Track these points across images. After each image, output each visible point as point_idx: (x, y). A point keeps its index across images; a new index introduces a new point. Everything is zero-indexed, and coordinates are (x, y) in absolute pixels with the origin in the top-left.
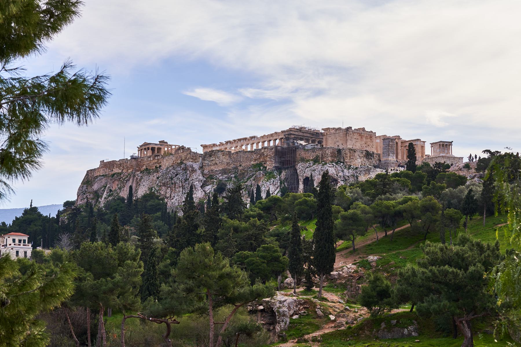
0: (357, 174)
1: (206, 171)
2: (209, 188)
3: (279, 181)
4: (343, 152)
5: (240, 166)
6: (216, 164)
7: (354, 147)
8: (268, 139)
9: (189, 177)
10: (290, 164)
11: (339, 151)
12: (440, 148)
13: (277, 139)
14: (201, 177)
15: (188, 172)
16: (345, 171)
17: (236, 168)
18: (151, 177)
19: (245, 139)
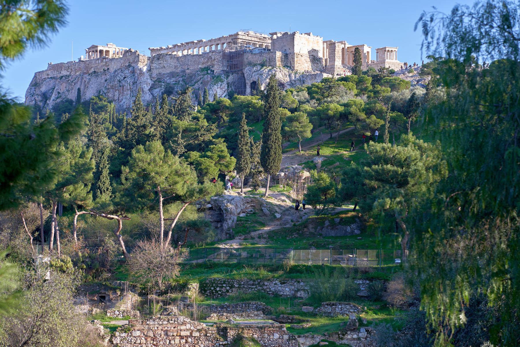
1: (154, 75)
2: (157, 92)
3: (226, 85)
4: (290, 57)
5: (188, 69)
6: (164, 67)
7: (301, 53)
8: (216, 43)
9: (137, 80)
10: (237, 67)
13: (224, 43)
14: (149, 81)
15: (136, 75)
17: (184, 71)
18: (99, 80)
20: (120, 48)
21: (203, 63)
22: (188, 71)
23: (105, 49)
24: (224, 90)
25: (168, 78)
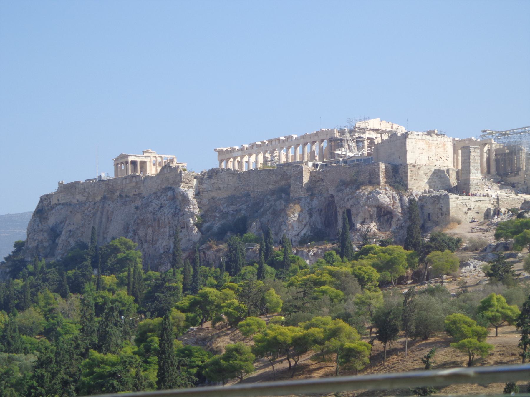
6: (219, 189)
7: (418, 162)
8: (312, 140)
15: (178, 203)
20: (163, 156)
21: (275, 183)
23: (139, 160)
24: (303, 223)
25: (225, 205)
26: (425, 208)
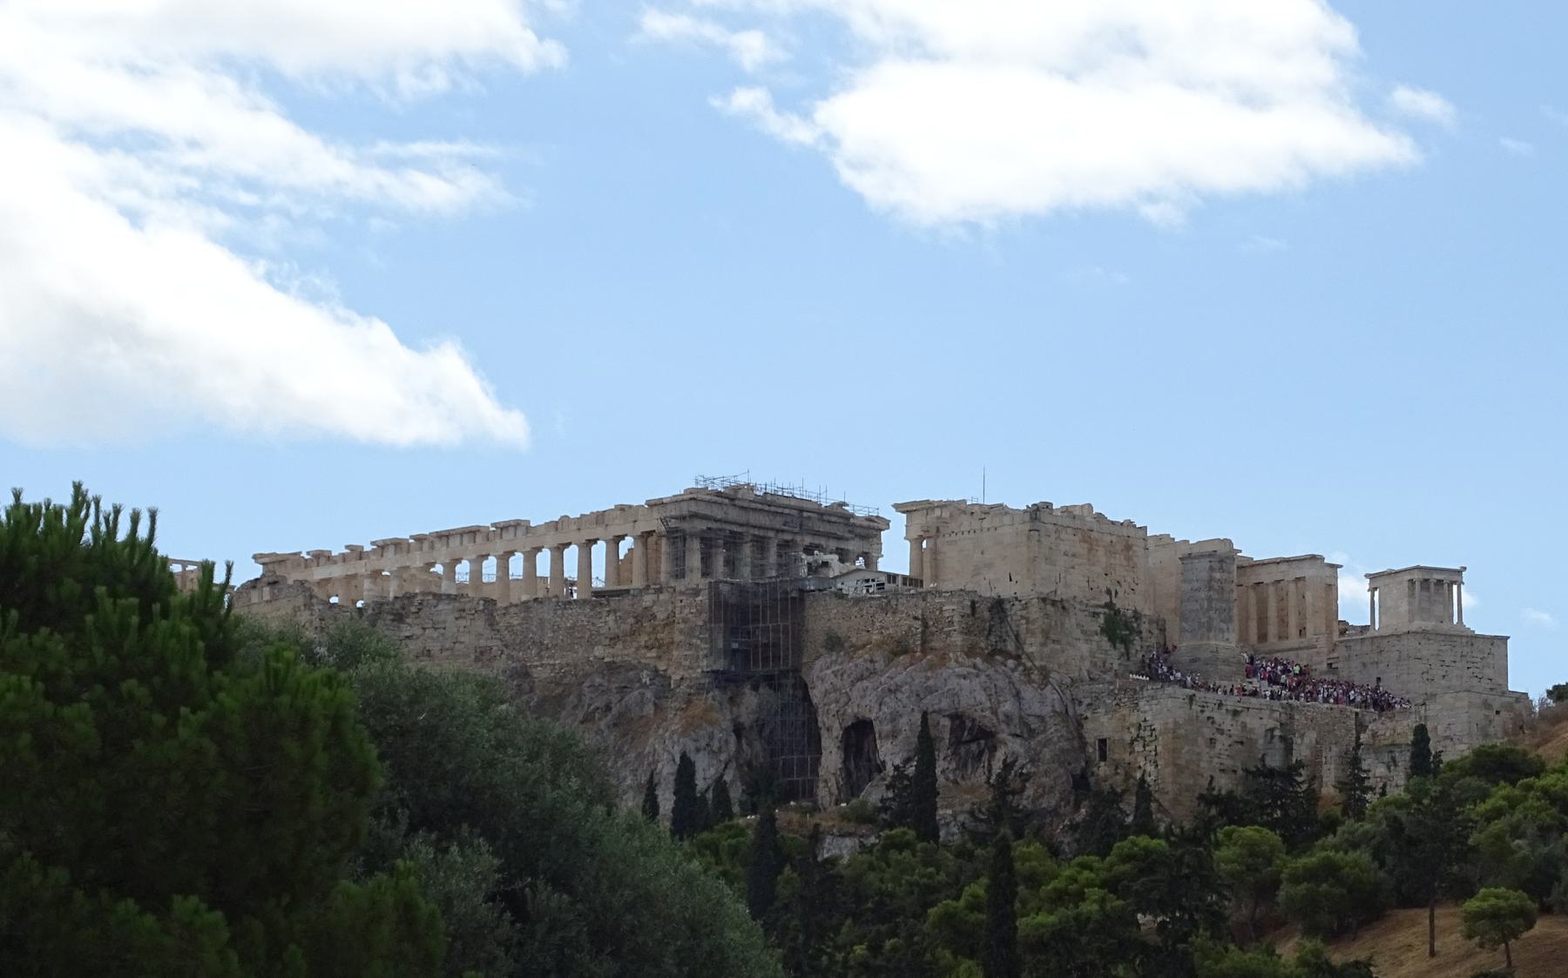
0: (1081, 710)
4: (1015, 612)
7: (1062, 593)
10: (776, 658)
11: (998, 605)
12: (1412, 595)
16: (1028, 693)
17: (524, 674)
19: (473, 532)
21: (614, 639)
22: (541, 674)
24: (723, 757)
26: (1088, 726)
